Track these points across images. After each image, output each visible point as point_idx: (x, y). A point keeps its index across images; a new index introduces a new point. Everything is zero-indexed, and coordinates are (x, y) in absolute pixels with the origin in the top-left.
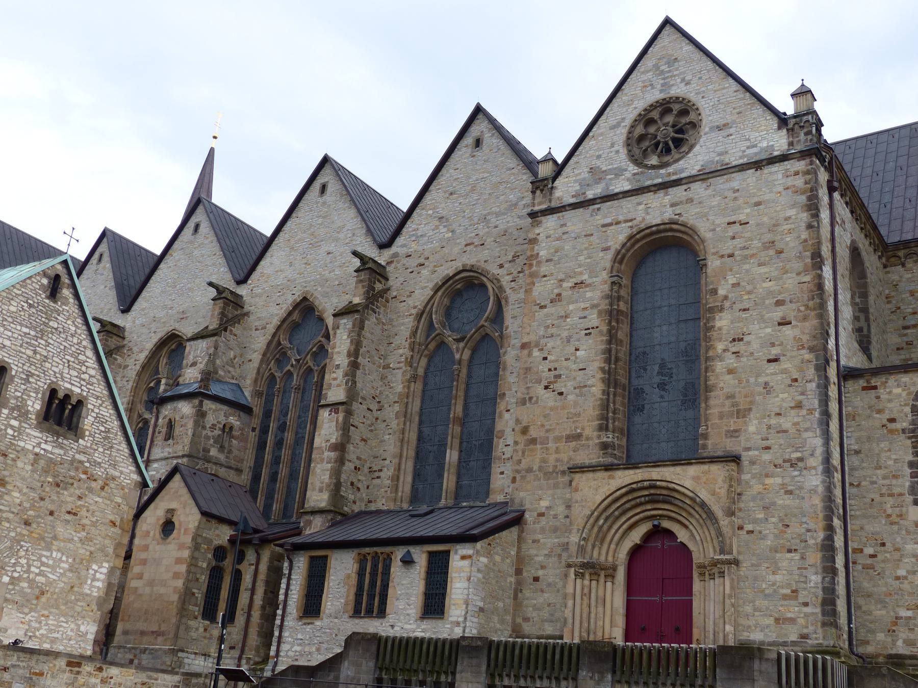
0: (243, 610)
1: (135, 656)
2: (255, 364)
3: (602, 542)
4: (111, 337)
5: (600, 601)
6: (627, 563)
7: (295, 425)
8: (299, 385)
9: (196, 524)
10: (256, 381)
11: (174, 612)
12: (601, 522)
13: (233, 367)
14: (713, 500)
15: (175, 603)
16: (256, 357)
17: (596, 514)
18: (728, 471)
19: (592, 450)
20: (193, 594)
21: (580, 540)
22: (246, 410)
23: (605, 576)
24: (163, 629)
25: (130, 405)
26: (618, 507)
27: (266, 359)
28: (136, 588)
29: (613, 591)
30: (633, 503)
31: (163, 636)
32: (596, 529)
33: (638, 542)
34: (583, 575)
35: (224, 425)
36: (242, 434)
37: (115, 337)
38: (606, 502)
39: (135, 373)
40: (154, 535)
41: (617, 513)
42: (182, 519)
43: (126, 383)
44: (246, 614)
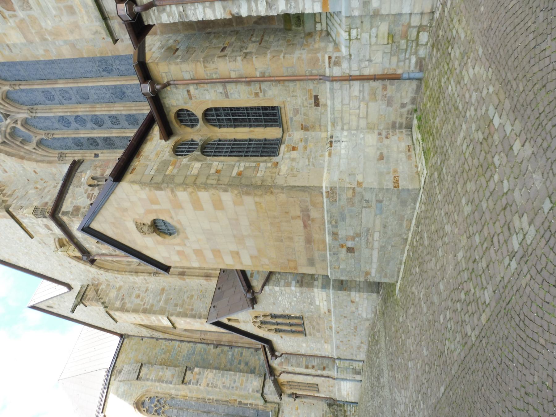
0: (257, 94)
1: (342, 246)
2: (34, 165)
4: (87, 296)
7: (70, 106)
8: (28, 109)
9: (136, 187)
10: (50, 162)
11: (268, 198)
13: (45, 188)
15: (257, 199)
16: (29, 166)
20: (240, 174)
22: (75, 166)
24: (299, 213)
25: (133, 273)
27: (27, 156)
28: (251, 257)
31: (308, 210)
35: (90, 185)
36: (100, 167)
37: (87, 293)
39: (107, 273)
40: (179, 244)
42: (141, 211)
43: (119, 279)
44: (264, 86)
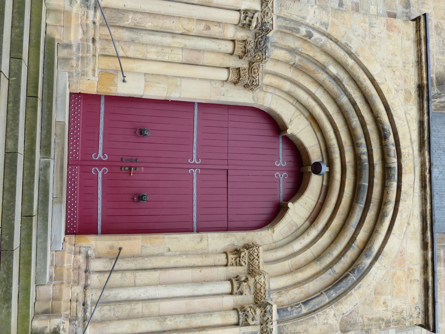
3: (295, 67)
5: (193, 57)
6: (254, 106)
12: (334, 69)
14: (368, 292)
17: (350, 62)
18: (411, 316)
19: (438, 59)
21: (307, 25)
23: (238, 69)
26: (354, 104)
29: (211, 80)
30: (359, 131)
32: (322, 58)
33: (289, 132)
34: (246, 26)
38: (367, 83)
41: (344, 100)
